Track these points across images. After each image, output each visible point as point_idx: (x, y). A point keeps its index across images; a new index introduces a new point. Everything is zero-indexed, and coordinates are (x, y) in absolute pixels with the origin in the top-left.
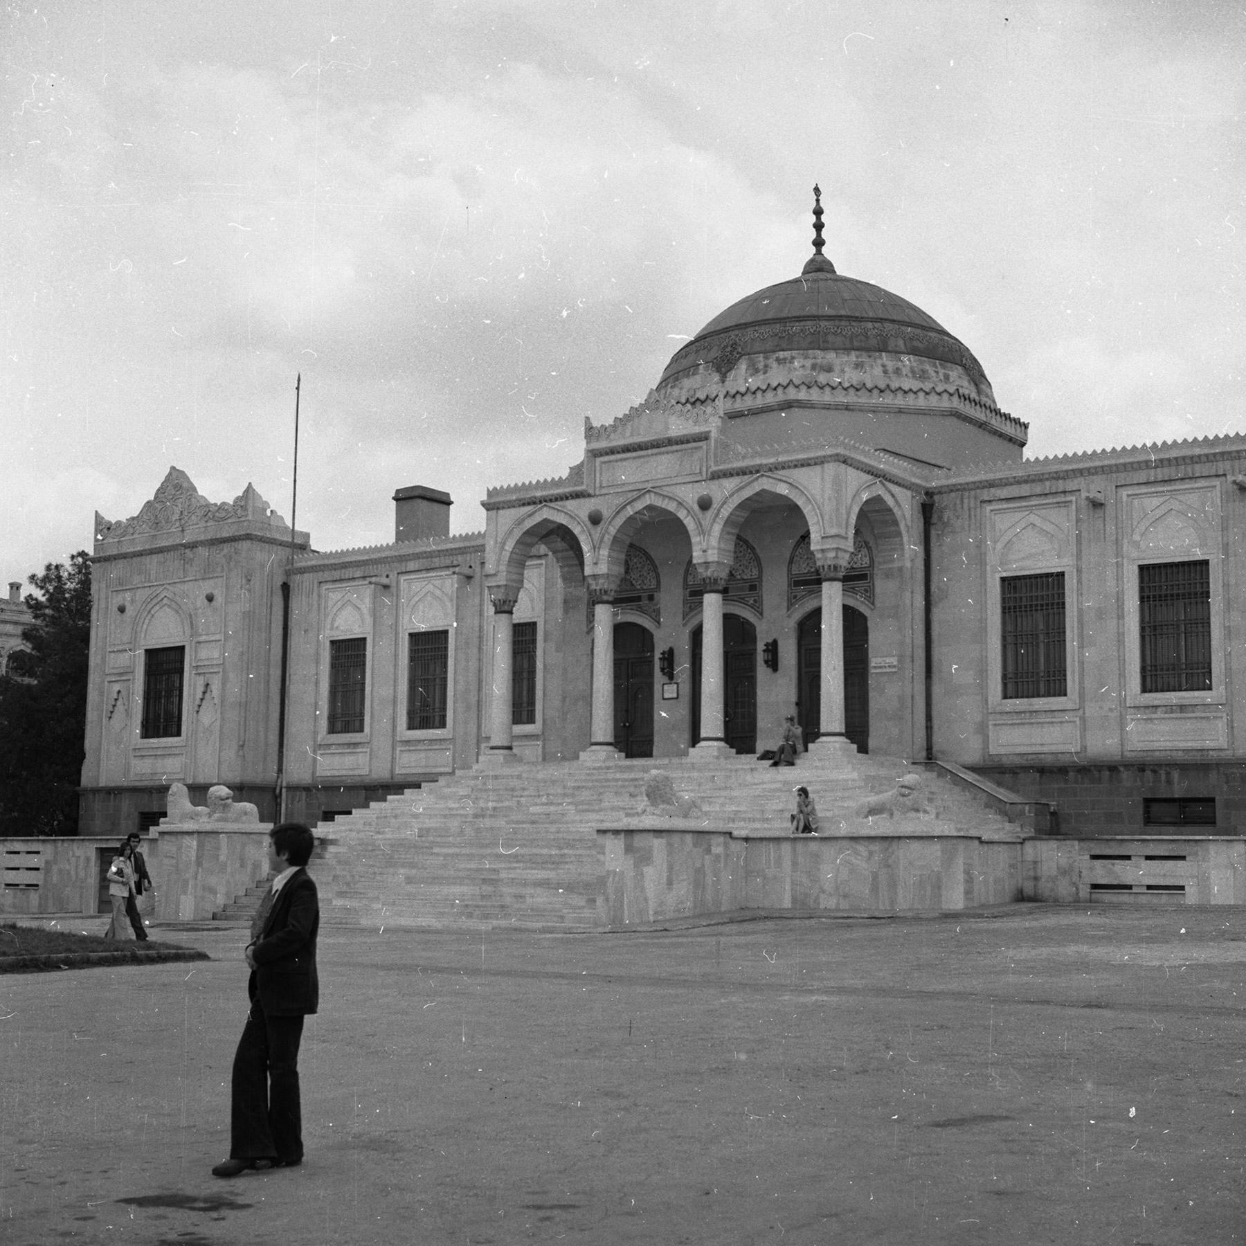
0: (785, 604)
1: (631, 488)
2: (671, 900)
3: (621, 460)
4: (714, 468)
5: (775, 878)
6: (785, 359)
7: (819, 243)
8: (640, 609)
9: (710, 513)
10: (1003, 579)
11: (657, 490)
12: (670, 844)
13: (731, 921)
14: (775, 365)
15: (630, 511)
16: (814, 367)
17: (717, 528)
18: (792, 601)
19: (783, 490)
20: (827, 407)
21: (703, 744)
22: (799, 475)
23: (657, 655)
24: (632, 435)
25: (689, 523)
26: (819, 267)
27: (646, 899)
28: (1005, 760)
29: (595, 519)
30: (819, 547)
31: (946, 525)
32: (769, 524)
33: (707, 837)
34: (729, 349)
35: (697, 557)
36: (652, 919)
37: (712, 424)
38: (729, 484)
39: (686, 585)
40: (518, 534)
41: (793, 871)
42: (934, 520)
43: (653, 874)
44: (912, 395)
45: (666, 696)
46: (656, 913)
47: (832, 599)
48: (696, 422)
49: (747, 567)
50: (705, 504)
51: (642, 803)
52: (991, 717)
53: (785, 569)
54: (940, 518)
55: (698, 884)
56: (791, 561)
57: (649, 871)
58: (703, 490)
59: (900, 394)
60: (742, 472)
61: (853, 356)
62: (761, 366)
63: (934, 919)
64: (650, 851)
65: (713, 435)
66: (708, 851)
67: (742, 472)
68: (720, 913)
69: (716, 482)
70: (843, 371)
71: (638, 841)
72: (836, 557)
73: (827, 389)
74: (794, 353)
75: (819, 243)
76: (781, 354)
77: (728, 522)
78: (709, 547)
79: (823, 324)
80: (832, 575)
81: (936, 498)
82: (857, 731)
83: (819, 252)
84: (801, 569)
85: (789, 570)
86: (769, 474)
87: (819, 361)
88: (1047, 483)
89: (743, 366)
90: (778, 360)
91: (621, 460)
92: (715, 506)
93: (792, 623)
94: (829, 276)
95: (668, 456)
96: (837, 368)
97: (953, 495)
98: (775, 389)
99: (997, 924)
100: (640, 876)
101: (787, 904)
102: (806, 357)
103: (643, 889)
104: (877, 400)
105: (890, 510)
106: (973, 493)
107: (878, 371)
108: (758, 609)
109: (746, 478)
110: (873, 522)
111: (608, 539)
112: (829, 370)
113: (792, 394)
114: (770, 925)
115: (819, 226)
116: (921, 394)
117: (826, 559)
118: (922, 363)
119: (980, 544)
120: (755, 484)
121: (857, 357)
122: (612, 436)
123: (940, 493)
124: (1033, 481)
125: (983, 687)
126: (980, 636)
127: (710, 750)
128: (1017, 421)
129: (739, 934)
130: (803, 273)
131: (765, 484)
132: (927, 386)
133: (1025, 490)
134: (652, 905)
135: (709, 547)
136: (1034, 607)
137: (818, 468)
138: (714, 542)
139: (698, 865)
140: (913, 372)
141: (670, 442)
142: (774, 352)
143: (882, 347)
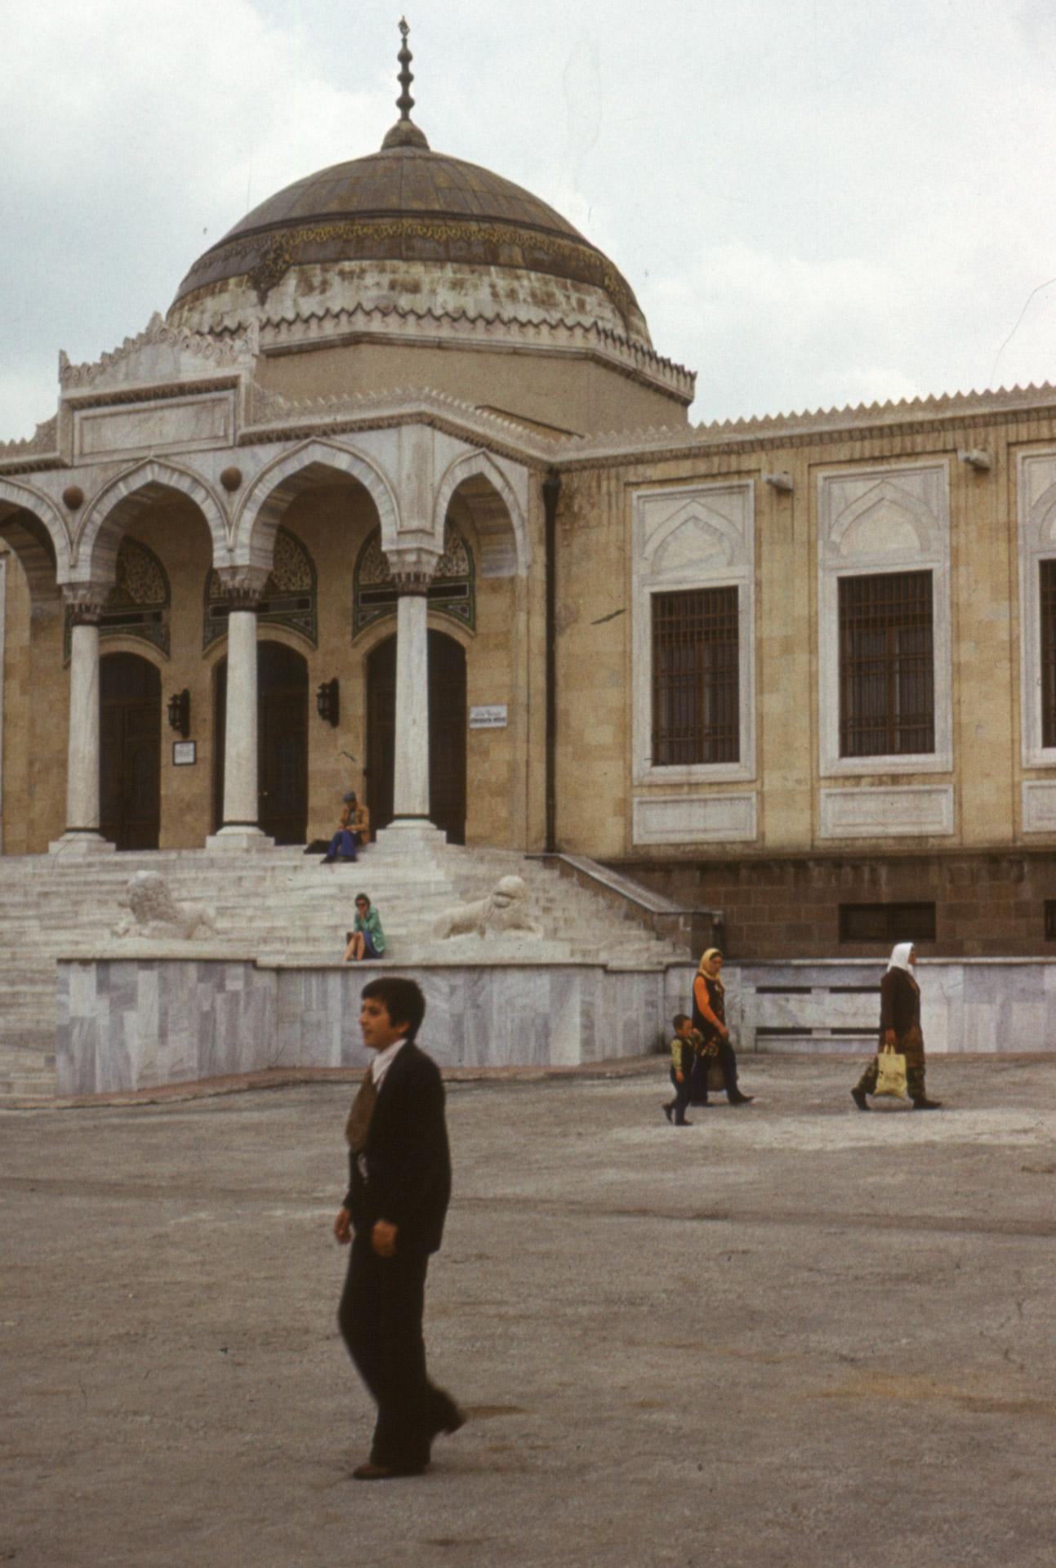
0: (350, 629)
1: (126, 457)
2: (164, 1059)
3: (112, 415)
4: (244, 430)
5: (319, 1024)
6: (352, 273)
7: (405, 103)
8: (140, 632)
9: (238, 497)
10: (656, 597)
11: (162, 461)
12: (163, 979)
13: (252, 1088)
14: (335, 280)
15: (123, 490)
16: (393, 286)
17: (249, 517)
18: (360, 624)
19: (342, 462)
20: (410, 344)
21: (225, 830)
22: (367, 442)
23: (166, 701)
24: (127, 376)
25: (209, 510)
26: (406, 138)
27: (127, 1058)
28: (654, 852)
30: (393, 547)
31: (576, 517)
32: (323, 514)
33: (219, 967)
34: (272, 255)
35: (220, 557)
36: (135, 1086)
37: (241, 363)
38: (268, 453)
39: (207, 599)
41: (344, 1014)
42: (561, 508)
43: (139, 1023)
44: (531, 330)
45: (178, 760)
46: (142, 1077)
47: (412, 623)
48: (219, 363)
49: (295, 574)
50: (231, 481)
51: (126, 919)
52: (637, 791)
53: (350, 577)
54: (569, 507)
55: (206, 1035)
56: (358, 567)
57: (132, 1019)
59: (515, 327)
60: (284, 436)
61: (449, 271)
62: (316, 281)
63: (537, 1082)
64: (134, 987)
65: (245, 380)
66: (221, 987)
67: (284, 436)
68: (237, 1076)
69: (246, 452)
70: (433, 292)
71: (116, 974)
72: (418, 562)
73: (411, 319)
74: (366, 263)
75: (405, 103)
76: (347, 265)
77: (266, 508)
78: (237, 545)
79: (407, 222)
80: (412, 587)
81: (564, 478)
82: (449, 811)
83: (405, 117)
85: (356, 579)
86: (324, 440)
87: (400, 277)
88: (716, 460)
89: (291, 283)
90: (342, 273)
91: (112, 415)
92: (246, 483)
93: (358, 655)
94: (419, 152)
95: (182, 411)
96: (426, 288)
97: (586, 474)
98: (307, 321)
99: (620, 1089)
100: (118, 1026)
101: (335, 1061)
102: (382, 270)
103: (122, 1044)
104: (479, 335)
105: (496, 494)
106: (613, 471)
107: (485, 293)
108: (310, 633)
109: (291, 445)
110: (473, 512)
112: (415, 289)
113: (360, 324)
114: (303, 1093)
116: (544, 329)
117: (403, 563)
118: (546, 283)
119: (623, 547)
120: (303, 454)
121: (455, 272)
122: (97, 381)
123: (568, 471)
124: (696, 456)
125: (625, 747)
126: (625, 675)
127: (236, 839)
128: (679, 370)
129: (260, 1107)
130: (387, 146)
131: (316, 454)
132: (554, 316)
133: (684, 468)
134: (136, 1062)
135: (237, 545)
136: (697, 636)
137: (392, 434)
138: (244, 537)
139: (206, 1007)
140: (533, 295)
141: (182, 390)
142: (337, 260)
143: (491, 257)
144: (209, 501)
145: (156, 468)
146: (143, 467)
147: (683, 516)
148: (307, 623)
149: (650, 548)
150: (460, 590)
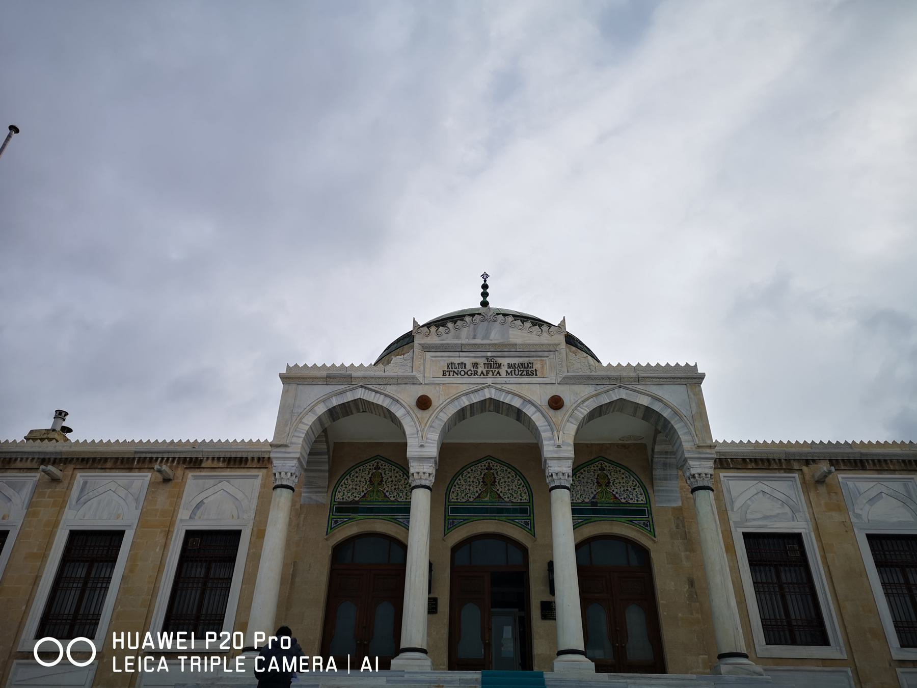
4: (566, 374)
25: (538, 419)
29: (424, 403)
40: (321, 409)
50: (556, 403)
109: (601, 388)
111: (439, 426)
144: (538, 414)
145: (493, 391)
146: (482, 389)
147: (753, 491)
148: (526, 523)
149: (737, 505)
150: (642, 512)
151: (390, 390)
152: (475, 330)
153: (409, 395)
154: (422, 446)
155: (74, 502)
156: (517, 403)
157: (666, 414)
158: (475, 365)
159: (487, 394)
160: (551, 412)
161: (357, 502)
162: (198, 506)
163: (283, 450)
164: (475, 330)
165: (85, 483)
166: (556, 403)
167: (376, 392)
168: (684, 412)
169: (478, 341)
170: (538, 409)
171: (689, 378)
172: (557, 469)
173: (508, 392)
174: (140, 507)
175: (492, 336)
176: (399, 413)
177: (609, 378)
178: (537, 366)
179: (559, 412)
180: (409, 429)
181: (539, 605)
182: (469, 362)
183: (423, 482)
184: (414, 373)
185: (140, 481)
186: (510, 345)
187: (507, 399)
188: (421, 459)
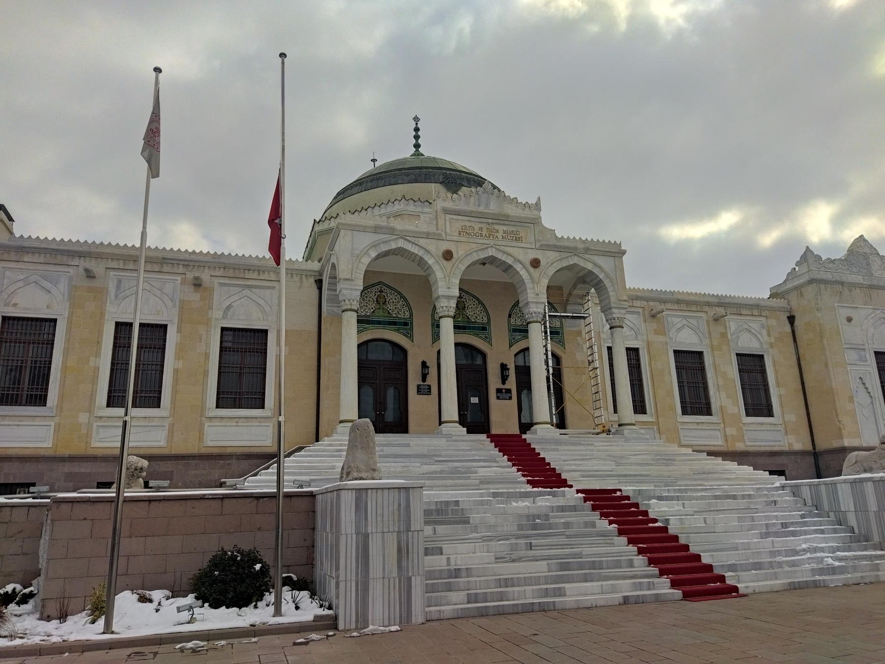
7: (417, 146)
19: (589, 266)
25: (523, 273)
38: (552, 255)
50: (536, 263)
56: (510, 316)
58: (532, 255)
75: (417, 146)
83: (417, 150)
84: (516, 321)
85: (509, 322)
109: (563, 255)
115: (417, 137)
146: (487, 248)
151: (422, 242)
152: (479, 199)
153: (437, 248)
154: (449, 288)
155: (113, 297)
156: (510, 261)
157: (601, 276)
158: (481, 229)
159: (491, 252)
160: (532, 270)
161: (369, 316)
162: (229, 307)
163: (350, 282)
164: (479, 199)
165: (120, 282)
166: (536, 263)
167: (413, 243)
168: (612, 275)
169: (481, 209)
170: (524, 267)
171: (616, 252)
172: (535, 310)
173: (504, 252)
174: (177, 305)
175: (491, 208)
176: (431, 261)
177: (568, 248)
178: (522, 234)
179: (537, 270)
180: (439, 274)
181: (495, 391)
182: (477, 227)
183: (446, 313)
184: (439, 231)
185: (173, 284)
186: (505, 215)
187: (503, 258)
188: (449, 297)
